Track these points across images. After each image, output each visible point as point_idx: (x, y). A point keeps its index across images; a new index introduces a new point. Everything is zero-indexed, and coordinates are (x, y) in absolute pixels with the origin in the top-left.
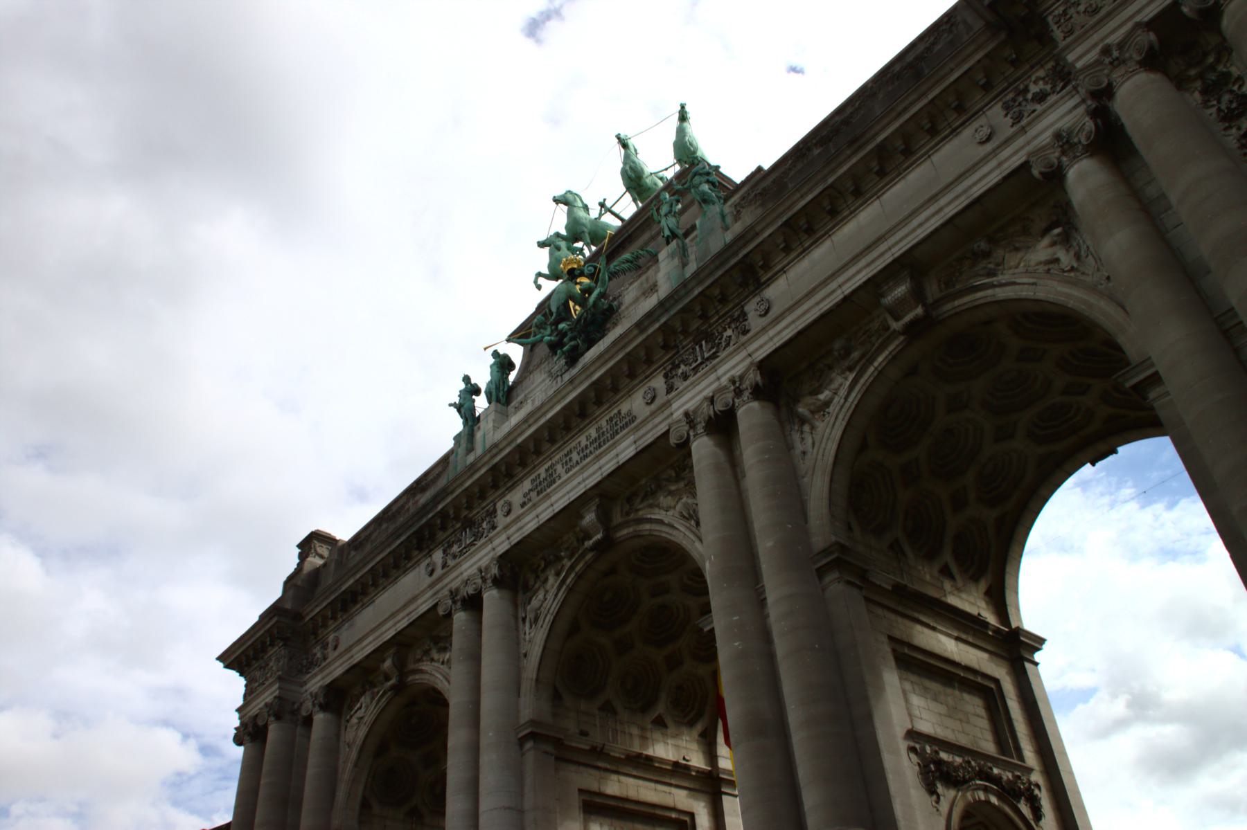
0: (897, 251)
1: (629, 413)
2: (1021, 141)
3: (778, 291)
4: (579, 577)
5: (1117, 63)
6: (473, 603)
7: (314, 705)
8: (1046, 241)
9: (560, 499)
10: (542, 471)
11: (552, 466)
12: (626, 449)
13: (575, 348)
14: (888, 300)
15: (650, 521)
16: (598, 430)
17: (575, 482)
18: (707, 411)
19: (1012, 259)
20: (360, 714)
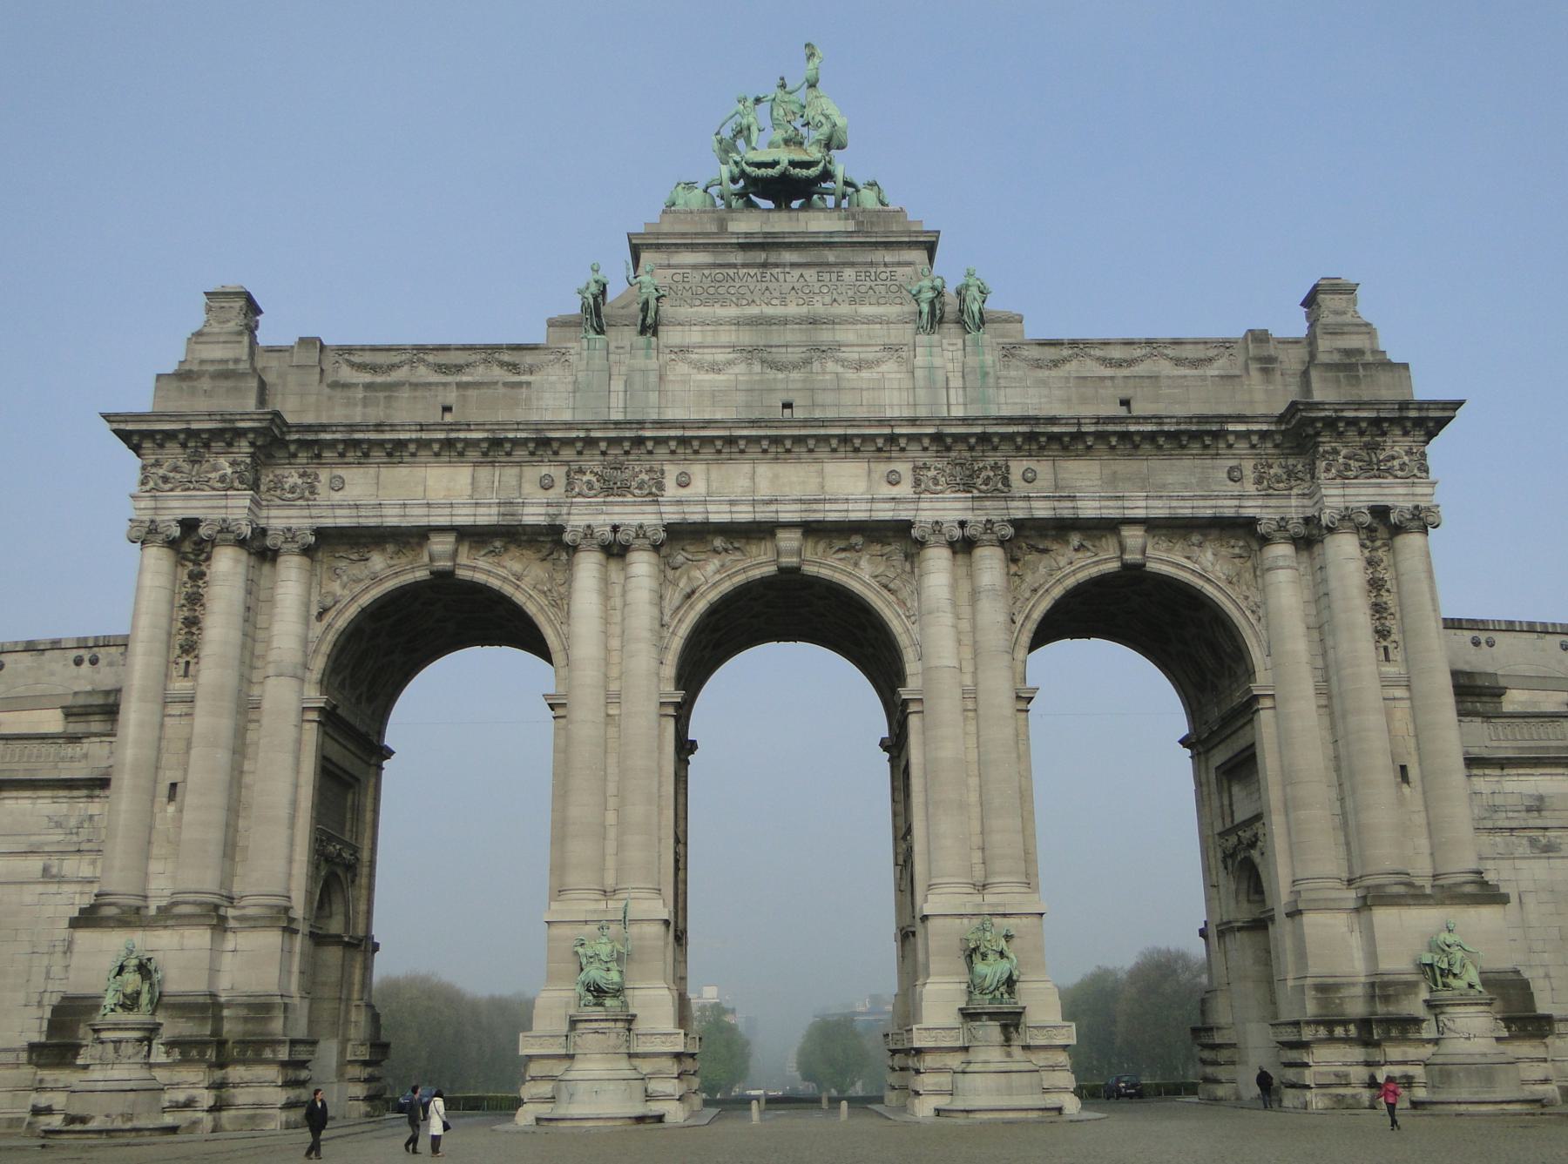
6: (616, 550)
18: (957, 533)
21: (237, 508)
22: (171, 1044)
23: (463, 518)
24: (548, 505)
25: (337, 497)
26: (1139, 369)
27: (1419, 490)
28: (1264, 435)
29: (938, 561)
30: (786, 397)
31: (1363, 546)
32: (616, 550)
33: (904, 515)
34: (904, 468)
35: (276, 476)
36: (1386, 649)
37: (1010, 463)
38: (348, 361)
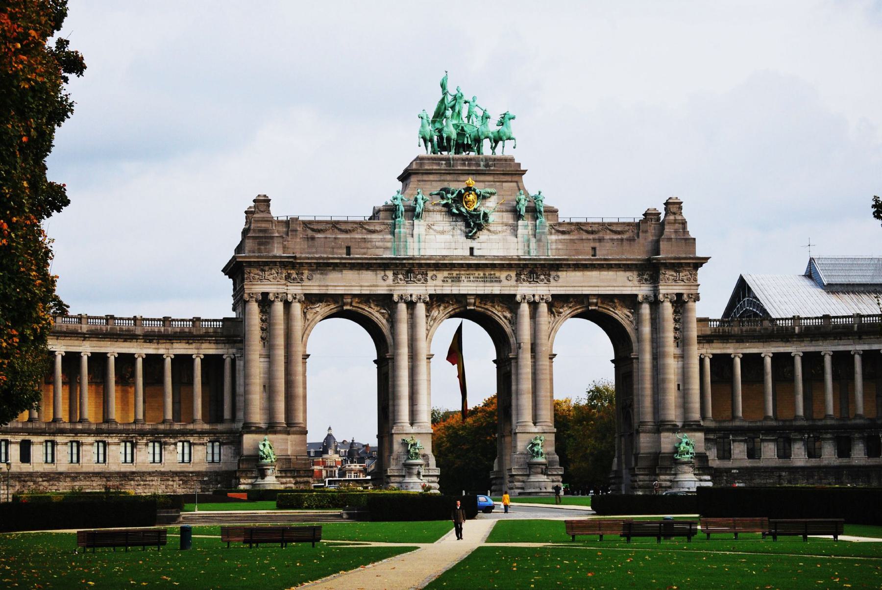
0: (600, 293)
1: (499, 278)
2: (638, 288)
3: (562, 274)
4: (455, 312)
5: (667, 298)
6: (411, 305)
7: (295, 298)
8: (628, 310)
9: (463, 291)
10: (455, 273)
11: (460, 274)
12: (496, 289)
13: (476, 233)
14: (591, 301)
15: (492, 312)
16: (484, 274)
17: (472, 288)
19: (619, 307)
20: (318, 309)
21: (281, 289)
22: (281, 471)
23: (356, 291)
24: (388, 286)
25: (310, 283)
26: (601, 235)
27: (692, 288)
28: (641, 264)
29: (525, 309)
30: (472, 246)
31: (673, 305)
32: (411, 305)
33: (512, 292)
34: (513, 274)
35: (289, 274)
36: (677, 343)
37: (551, 273)
38: (309, 228)
